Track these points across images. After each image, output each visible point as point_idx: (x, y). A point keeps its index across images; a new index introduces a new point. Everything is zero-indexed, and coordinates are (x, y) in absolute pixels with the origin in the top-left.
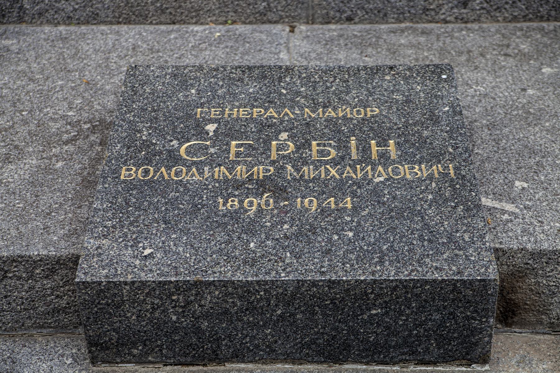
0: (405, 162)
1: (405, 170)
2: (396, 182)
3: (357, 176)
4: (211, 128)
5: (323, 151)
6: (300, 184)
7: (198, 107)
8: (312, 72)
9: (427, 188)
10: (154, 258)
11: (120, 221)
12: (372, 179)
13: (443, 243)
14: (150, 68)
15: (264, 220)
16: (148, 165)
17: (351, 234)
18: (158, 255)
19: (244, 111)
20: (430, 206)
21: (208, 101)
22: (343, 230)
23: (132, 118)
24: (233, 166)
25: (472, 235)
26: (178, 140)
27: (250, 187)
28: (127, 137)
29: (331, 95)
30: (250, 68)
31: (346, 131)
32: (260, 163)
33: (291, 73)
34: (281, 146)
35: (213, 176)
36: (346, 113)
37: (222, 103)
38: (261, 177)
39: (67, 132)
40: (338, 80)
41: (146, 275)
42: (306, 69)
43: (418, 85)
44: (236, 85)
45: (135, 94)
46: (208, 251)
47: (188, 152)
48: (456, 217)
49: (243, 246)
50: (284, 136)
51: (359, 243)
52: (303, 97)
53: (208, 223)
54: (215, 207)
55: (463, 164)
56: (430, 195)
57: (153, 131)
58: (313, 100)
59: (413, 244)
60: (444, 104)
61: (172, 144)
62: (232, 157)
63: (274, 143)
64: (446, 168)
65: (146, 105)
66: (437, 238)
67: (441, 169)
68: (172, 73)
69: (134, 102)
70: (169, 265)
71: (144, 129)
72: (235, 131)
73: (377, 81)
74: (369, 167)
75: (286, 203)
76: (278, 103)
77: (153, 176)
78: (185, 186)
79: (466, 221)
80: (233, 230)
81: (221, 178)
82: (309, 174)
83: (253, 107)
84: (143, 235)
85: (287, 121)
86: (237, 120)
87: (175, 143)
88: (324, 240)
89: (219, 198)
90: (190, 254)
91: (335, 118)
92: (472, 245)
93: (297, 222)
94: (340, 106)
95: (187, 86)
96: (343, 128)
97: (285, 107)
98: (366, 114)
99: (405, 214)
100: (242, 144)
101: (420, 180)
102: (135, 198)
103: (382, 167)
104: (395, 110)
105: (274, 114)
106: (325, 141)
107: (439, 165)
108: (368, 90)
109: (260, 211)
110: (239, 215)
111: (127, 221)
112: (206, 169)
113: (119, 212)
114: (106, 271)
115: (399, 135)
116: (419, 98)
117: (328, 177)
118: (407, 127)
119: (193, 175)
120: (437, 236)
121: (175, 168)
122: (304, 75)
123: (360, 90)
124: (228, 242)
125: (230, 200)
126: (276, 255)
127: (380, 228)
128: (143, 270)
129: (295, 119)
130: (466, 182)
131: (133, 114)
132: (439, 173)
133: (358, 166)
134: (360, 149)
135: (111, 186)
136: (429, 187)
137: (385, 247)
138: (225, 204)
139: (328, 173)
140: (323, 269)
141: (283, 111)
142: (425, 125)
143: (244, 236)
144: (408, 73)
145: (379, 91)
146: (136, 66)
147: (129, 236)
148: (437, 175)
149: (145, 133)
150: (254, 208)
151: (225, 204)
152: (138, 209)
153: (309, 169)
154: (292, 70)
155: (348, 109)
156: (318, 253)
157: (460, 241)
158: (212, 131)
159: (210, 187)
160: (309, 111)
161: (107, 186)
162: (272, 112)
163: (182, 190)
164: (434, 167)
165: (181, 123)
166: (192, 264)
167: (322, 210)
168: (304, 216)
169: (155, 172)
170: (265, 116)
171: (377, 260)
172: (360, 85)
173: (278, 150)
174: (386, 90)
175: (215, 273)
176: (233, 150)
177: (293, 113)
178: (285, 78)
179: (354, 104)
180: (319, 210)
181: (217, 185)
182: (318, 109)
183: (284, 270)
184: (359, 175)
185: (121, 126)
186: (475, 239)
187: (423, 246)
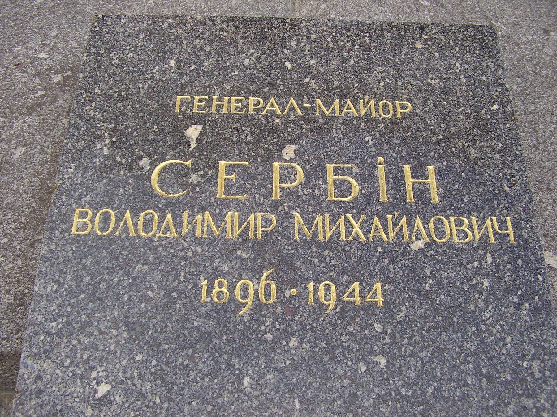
0: (450, 209)
1: (450, 226)
2: (440, 250)
3: (388, 238)
5: (342, 183)
6: (312, 252)
7: (177, 94)
8: (324, 31)
9: (480, 264)
10: (111, 403)
11: (69, 323)
12: (408, 245)
13: (507, 382)
14: (120, 19)
15: (263, 328)
16: (108, 205)
17: (383, 361)
18: (117, 398)
19: (237, 101)
20: (486, 301)
21: (190, 81)
22: (372, 352)
23: (92, 113)
24: (221, 210)
25: (542, 365)
26: (149, 156)
27: (245, 255)
28: (84, 148)
29: (349, 74)
30: (245, 22)
31: (370, 143)
33: (297, 32)
34: (286, 171)
35: (194, 229)
36: (370, 109)
37: (209, 86)
39: (34, 90)
40: (357, 47)
42: (316, 25)
43: (457, 61)
44: (226, 51)
45: (99, 67)
46: (186, 391)
47: (161, 181)
48: (521, 326)
49: (233, 383)
50: (289, 151)
51: (394, 381)
53: (186, 332)
55: (524, 216)
56: (486, 279)
57: (117, 139)
58: (326, 82)
59: (467, 385)
60: (492, 98)
61: (141, 163)
62: (220, 193)
63: (276, 164)
64: (502, 223)
65: (112, 89)
66: (498, 371)
67: (496, 226)
68: (147, 30)
69: (96, 83)
71: (106, 134)
72: (225, 139)
73: (406, 50)
74: (404, 219)
75: (294, 291)
76: (281, 87)
77: (115, 229)
78: (155, 250)
79: (533, 335)
81: (205, 236)
82: (324, 231)
83: (250, 93)
85: (293, 121)
86: (228, 118)
87: (145, 162)
88: (345, 373)
89: (202, 278)
90: (160, 398)
91: (356, 118)
92: (544, 386)
94: (361, 96)
95: (165, 53)
96: (367, 139)
97: (290, 95)
98: (395, 115)
99: (455, 319)
100: (234, 165)
101: (472, 248)
102: (89, 274)
103: (421, 219)
104: (431, 106)
105: (276, 108)
106: (343, 163)
107: (494, 218)
108: (395, 67)
109: (258, 307)
110: (228, 315)
111: (77, 323)
112: (185, 215)
113: (67, 302)
115: (440, 156)
116: (460, 85)
118: (449, 141)
119: (167, 229)
120: (499, 367)
121: (142, 214)
122: (314, 36)
123: (386, 66)
125: (216, 282)
126: (280, 404)
129: (303, 118)
130: (529, 253)
131: (94, 104)
132: (495, 233)
133: (389, 217)
134: (391, 180)
135: (59, 249)
136: (484, 263)
137: (430, 390)
138: (209, 292)
139: (350, 229)
141: (287, 103)
142: (471, 138)
143: (235, 361)
144: (443, 38)
145: (410, 70)
146: (103, 16)
147: (79, 355)
148: (492, 240)
150: (250, 301)
151: (209, 292)
152: (93, 297)
153: (324, 220)
154: (299, 25)
155: (372, 101)
156: (339, 402)
157: (528, 378)
158: (195, 139)
159: (190, 254)
160: (321, 103)
161: (53, 247)
162: (273, 103)
164: (488, 222)
165: (155, 123)
167: (343, 309)
168: (318, 321)
169: (118, 220)
170: (264, 113)
172: (385, 58)
173: (281, 181)
176: (222, 176)
177: (301, 107)
178: (289, 41)
179: (379, 91)
180: (338, 309)
181: (199, 250)
182: (333, 100)
184: (392, 235)
185: (78, 128)
186: (547, 373)
187: (481, 387)
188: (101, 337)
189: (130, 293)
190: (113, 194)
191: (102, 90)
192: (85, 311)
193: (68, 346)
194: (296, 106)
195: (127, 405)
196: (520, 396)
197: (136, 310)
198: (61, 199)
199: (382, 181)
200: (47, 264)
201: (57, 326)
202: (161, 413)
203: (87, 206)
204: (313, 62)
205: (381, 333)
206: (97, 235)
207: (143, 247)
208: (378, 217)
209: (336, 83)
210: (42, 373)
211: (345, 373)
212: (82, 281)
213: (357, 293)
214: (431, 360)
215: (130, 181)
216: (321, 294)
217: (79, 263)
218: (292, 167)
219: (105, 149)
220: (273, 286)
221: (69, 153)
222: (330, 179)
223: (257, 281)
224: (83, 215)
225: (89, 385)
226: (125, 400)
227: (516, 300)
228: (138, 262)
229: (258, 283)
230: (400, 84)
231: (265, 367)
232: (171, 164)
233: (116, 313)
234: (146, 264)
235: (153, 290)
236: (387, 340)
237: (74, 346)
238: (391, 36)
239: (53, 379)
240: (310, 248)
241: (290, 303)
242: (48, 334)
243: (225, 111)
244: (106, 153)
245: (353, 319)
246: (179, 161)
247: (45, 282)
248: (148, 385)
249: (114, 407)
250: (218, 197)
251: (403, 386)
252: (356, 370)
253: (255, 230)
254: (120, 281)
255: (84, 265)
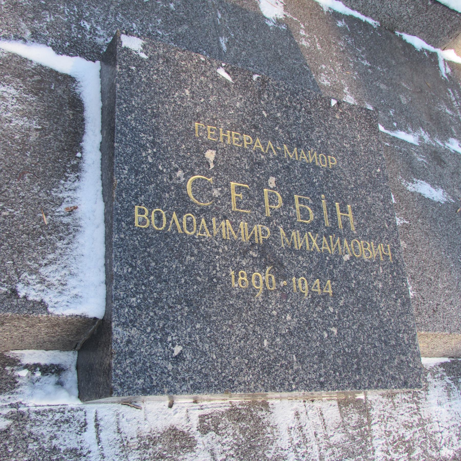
4: (210, 155)
9: (377, 272)
10: (184, 360)
11: (145, 299)
13: (393, 345)
17: (335, 330)
19: (236, 136)
22: (329, 325)
27: (255, 255)
31: (317, 184)
32: (258, 220)
36: (314, 159)
38: (261, 242)
41: (181, 388)
45: (132, 82)
46: (231, 350)
49: (258, 344)
50: (272, 181)
52: (280, 128)
53: (226, 308)
54: (228, 282)
70: (200, 372)
71: (148, 145)
77: (167, 226)
79: (403, 319)
80: (247, 320)
84: (170, 323)
87: (180, 173)
88: (317, 338)
90: (216, 354)
91: (307, 164)
92: (409, 349)
93: (296, 312)
97: (268, 138)
102: (154, 261)
103: (347, 240)
105: (261, 146)
110: (250, 296)
111: (151, 299)
112: (214, 220)
114: (141, 381)
115: (353, 199)
117: (312, 250)
122: (277, 94)
123: (320, 128)
124: (246, 337)
126: (285, 358)
127: (354, 324)
128: (177, 379)
129: (278, 158)
132: (383, 254)
133: (331, 236)
137: (359, 349)
140: (322, 379)
143: (257, 328)
145: (334, 134)
149: (150, 151)
150: (261, 287)
158: (212, 161)
161: (122, 236)
163: (196, 252)
164: (379, 246)
166: (220, 371)
169: (168, 219)
171: (355, 366)
174: (338, 134)
175: (240, 384)
176: (234, 194)
181: (226, 249)
183: (294, 380)
184: (333, 249)
185: (124, 134)
186: (411, 341)
188: (170, 310)
189: (186, 277)
190: (161, 196)
191: (138, 104)
192: (155, 290)
193: (148, 317)
194: (272, 148)
195: (195, 361)
196: (400, 354)
197: (191, 290)
198: (122, 196)
199: (325, 212)
200: (120, 250)
201: (136, 301)
202: (217, 365)
203: (143, 204)
204: (279, 115)
205: (333, 313)
206: (154, 229)
207: (189, 243)
208: (325, 236)
209: (294, 134)
210: (131, 338)
211: (317, 338)
212: (149, 266)
213: (318, 286)
214: (358, 332)
215: (172, 188)
216: (300, 285)
217: (145, 251)
218: (275, 194)
219: (149, 158)
220: (273, 277)
221: (121, 156)
222: (298, 205)
223: (263, 274)
224: (142, 212)
225: (168, 347)
226: (193, 357)
227: (394, 297)
228: (187, 254)
229: (264, 275)
230: (329, 143)
231: (275, 333)
232: (199, 179)
233: (178, 293)
234: (193, 256)
235: (200, 276)
236: (336, 318)
237: (152, 317)
238: (322, 105)
239: (141, 342)
240: (291, 253)
241: (284, 291)
242: (131, 307)
243: (228, 142)
244: (150, 161)
245: (318, 302)
246: (203, 177)
247: (121, 265)
248: (207, 346)
249: (187, 363)
250: (233, 209)
251: (346, 347)
252: (323, 336)
253: (259, 238)
254: (177, 267)
255: (149, 253)
